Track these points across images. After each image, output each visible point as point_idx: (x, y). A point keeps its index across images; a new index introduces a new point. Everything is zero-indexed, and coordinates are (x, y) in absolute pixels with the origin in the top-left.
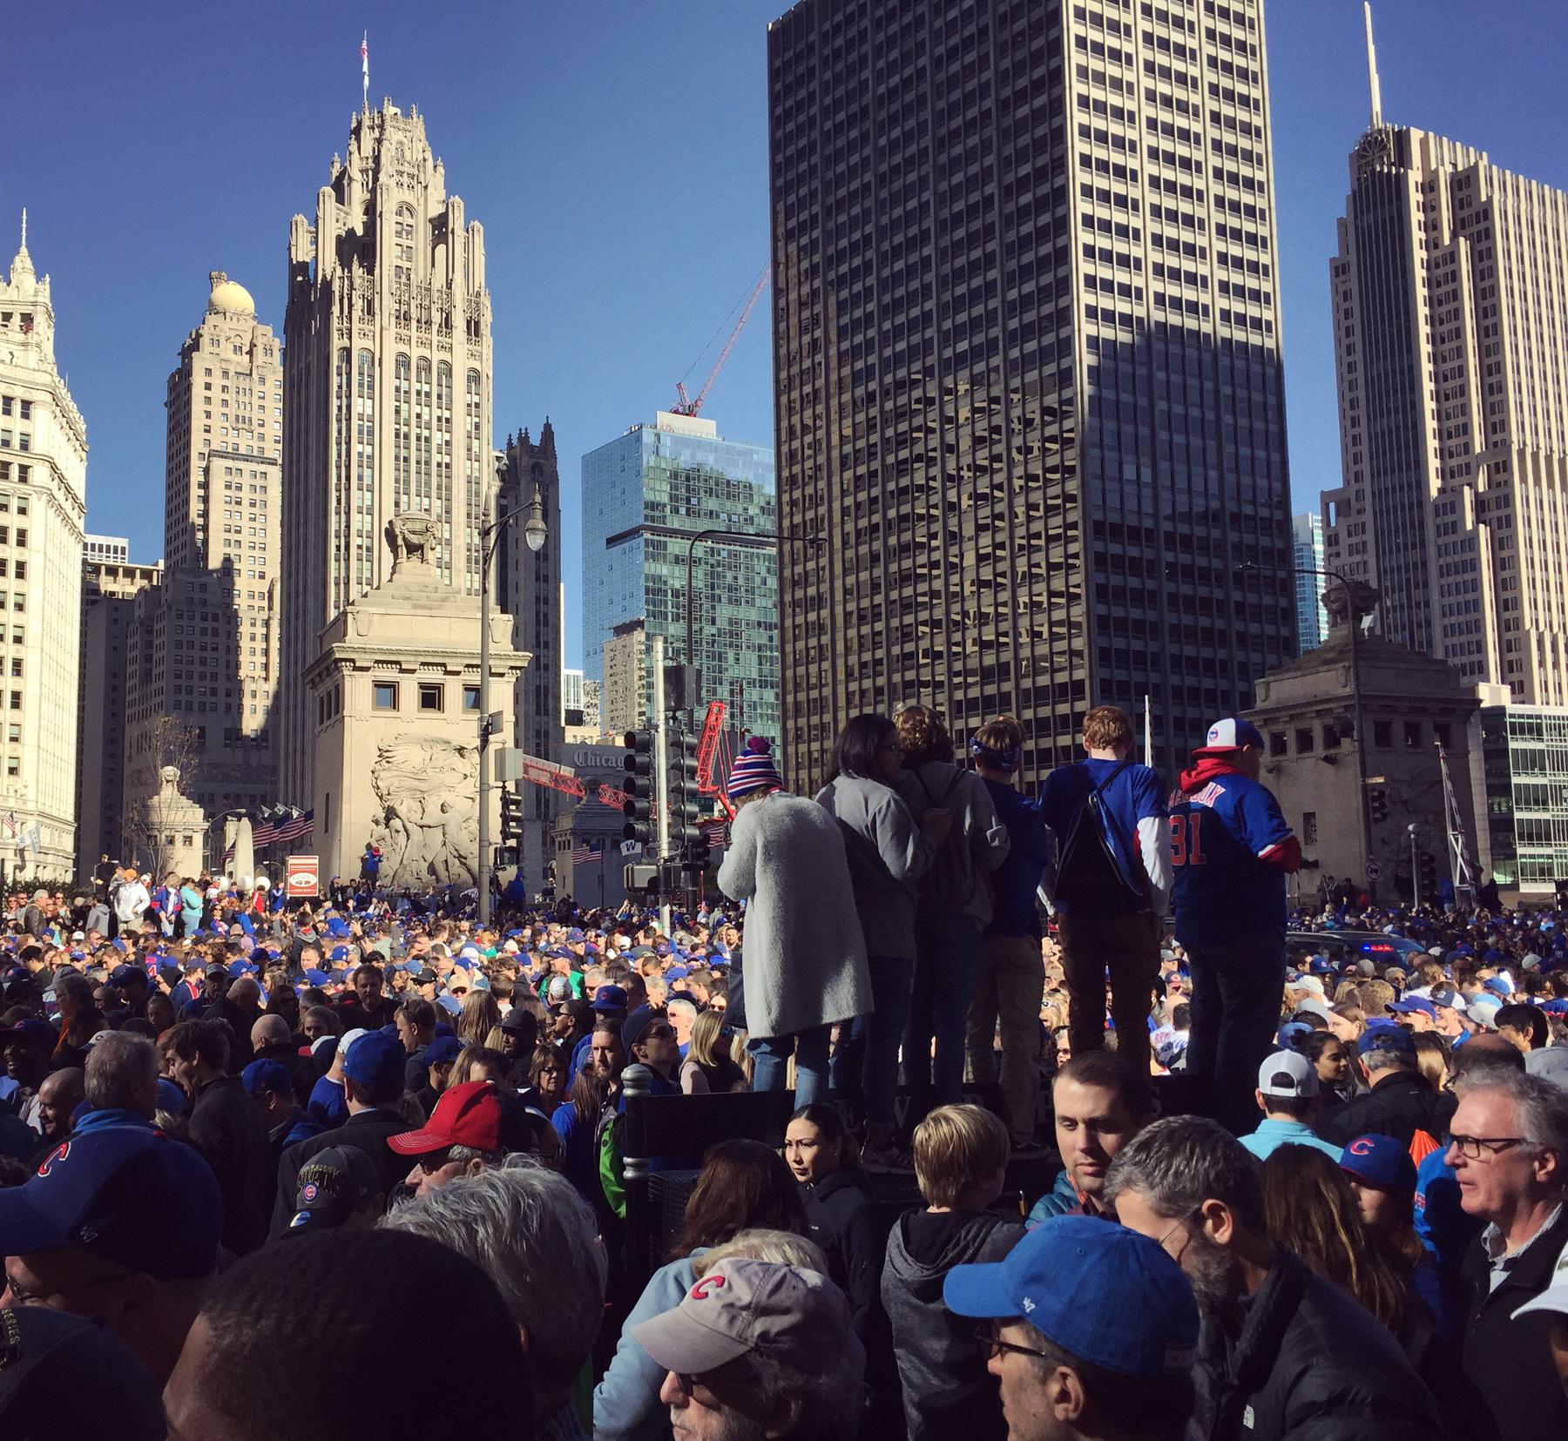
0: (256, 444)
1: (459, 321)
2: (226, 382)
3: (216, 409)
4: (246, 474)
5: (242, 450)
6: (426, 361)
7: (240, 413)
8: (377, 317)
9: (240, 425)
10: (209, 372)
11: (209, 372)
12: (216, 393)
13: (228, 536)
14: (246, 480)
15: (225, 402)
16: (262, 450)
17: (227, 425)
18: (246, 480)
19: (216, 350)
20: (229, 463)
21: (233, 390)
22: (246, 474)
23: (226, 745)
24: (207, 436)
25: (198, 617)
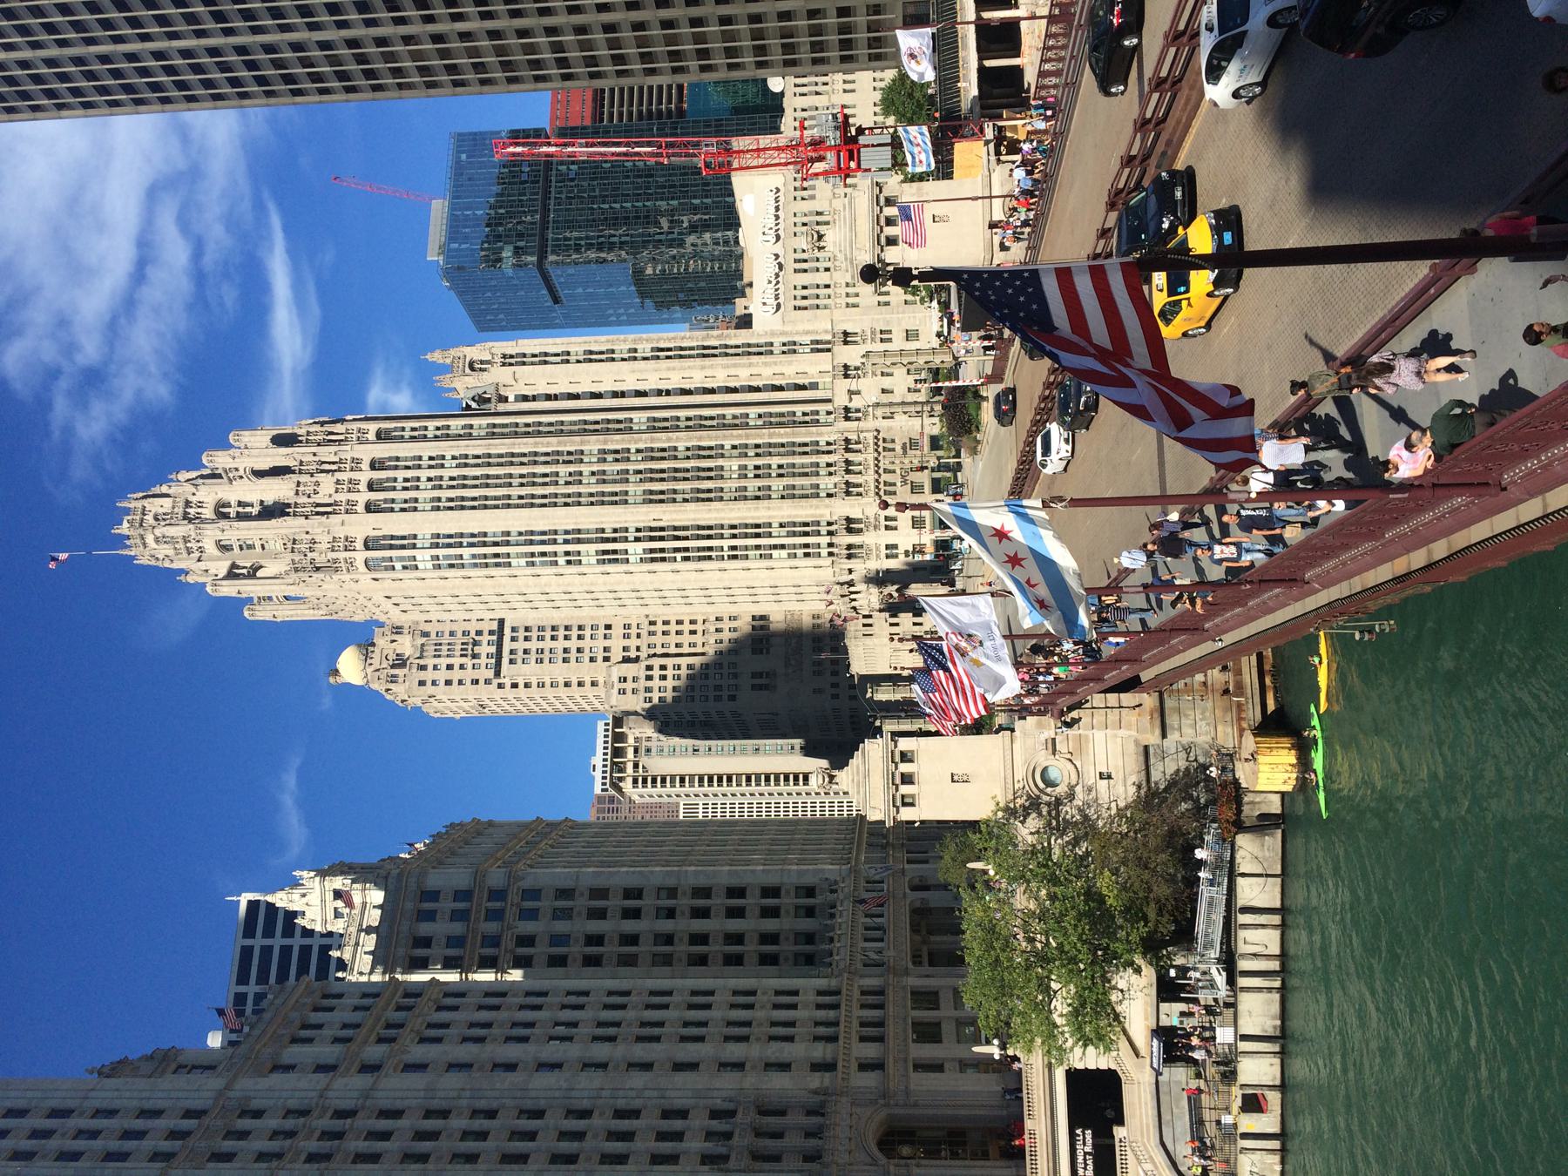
0: (485, 638)
2: (430, 668)
3: (456, 675)
4: (515, 645)
5: (493, 649)
7: (458, 653)
10: (422, 683)
11: (422, 683)
12: (442, 675)
13: (573, 660)
14: (520, 645)
15: (450, 667)
16: (491, 633)
18: (520, 645)
19: (401, 680)
20: (505, 661)
22: (515, 645)
23: (768, 652)
24: (482, 682)
25: (649, 684)
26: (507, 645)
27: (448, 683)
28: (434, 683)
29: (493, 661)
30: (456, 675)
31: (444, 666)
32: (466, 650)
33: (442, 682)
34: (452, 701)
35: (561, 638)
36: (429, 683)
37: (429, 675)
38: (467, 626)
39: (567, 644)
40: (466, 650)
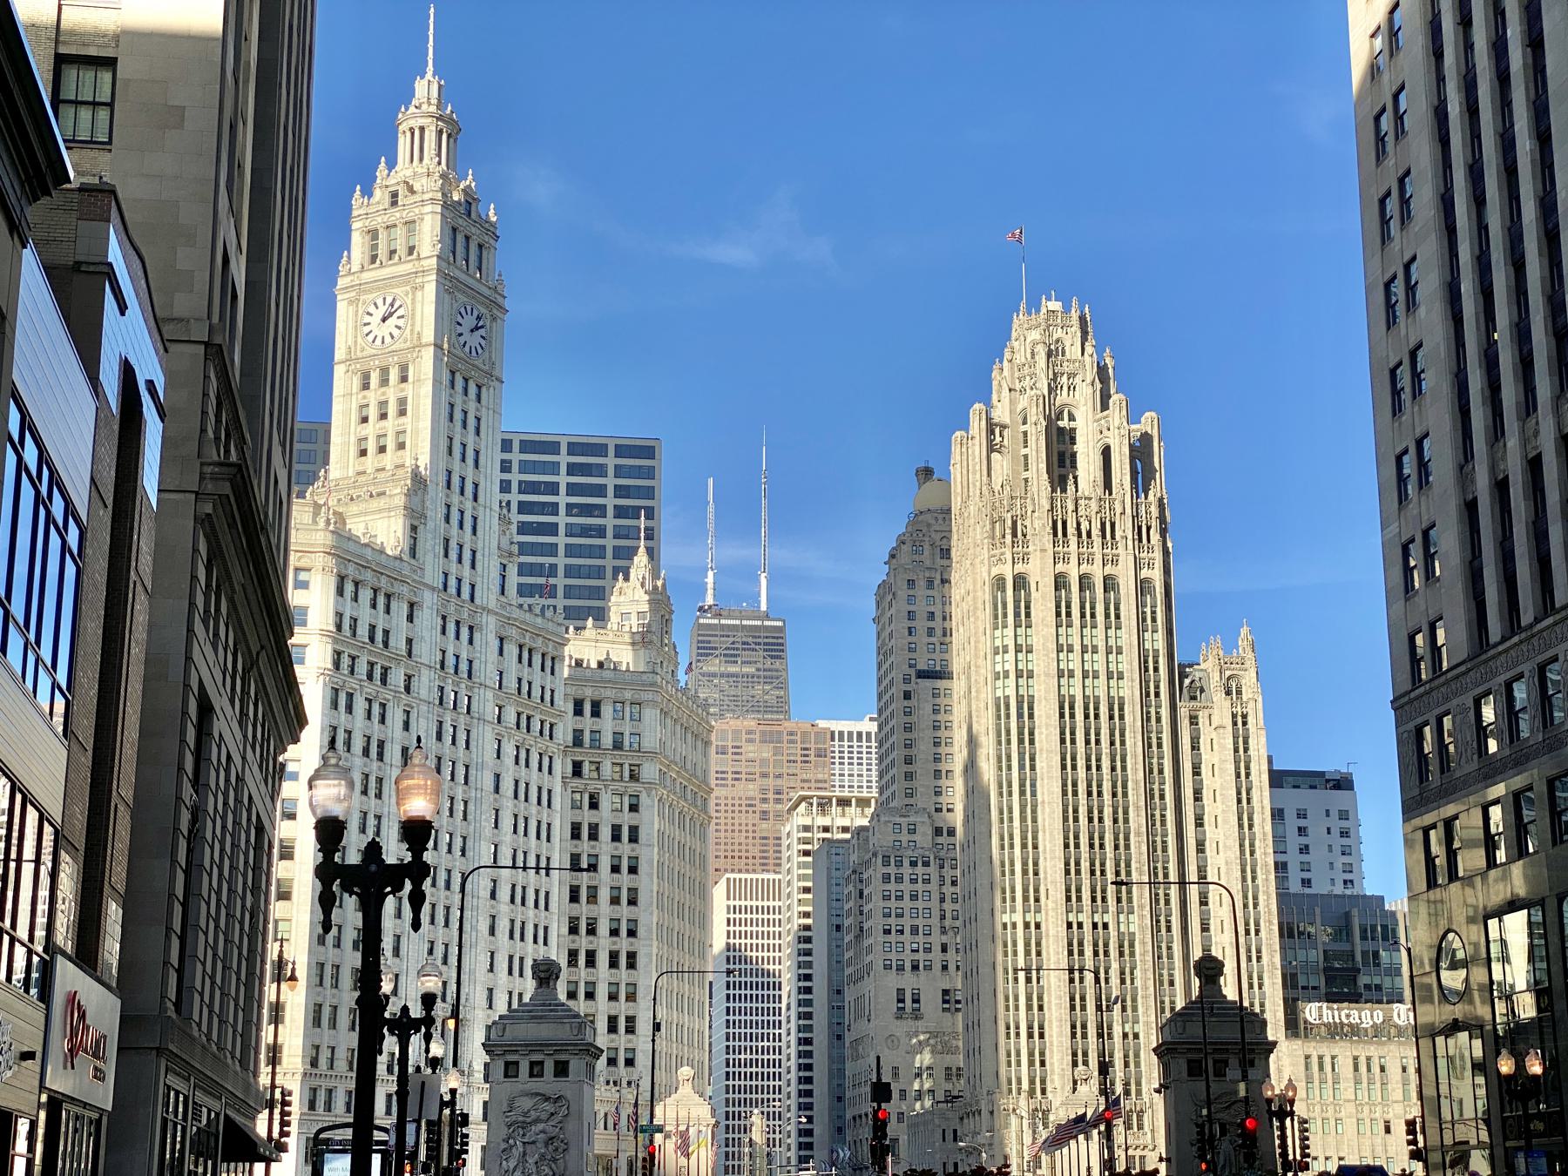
10: (911, 583)
11: (911, 583)
15: (931, 616)
19: (917, 557)
27: (911, 615)
28: (911, 599)
34: (891, 621)
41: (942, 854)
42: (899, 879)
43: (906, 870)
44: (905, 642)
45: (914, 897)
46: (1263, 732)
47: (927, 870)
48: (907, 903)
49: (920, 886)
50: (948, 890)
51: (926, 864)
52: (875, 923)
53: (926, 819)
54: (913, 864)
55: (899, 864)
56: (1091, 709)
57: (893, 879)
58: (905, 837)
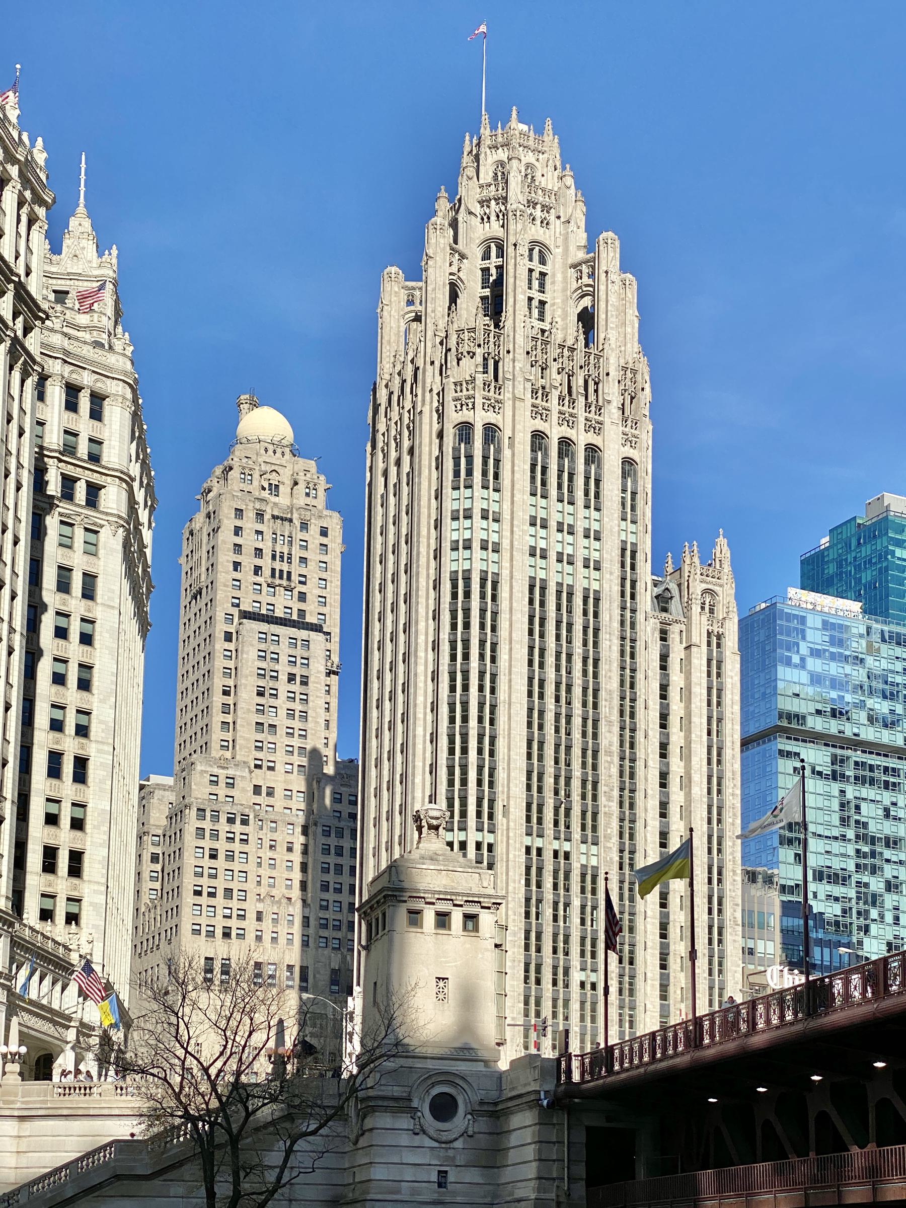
1: (611, 391)
2: (260, 527)
3: (248, 561)
4: (285, 642)
5: (279, 613)
6: (565, 444)
7: (278, 565)
8: (509, 384)
9: (277, 581)
10: (239, 512)
11: (239, 512)
12: (248, 541)
14: (284, 649)
15: (259, 552)
16: (302, 613)
17: (259, 579)
18: (284, 649)
20: (264, 627)
21: (268, 536)
26: (285, 632)
27: (238, 548)
28: (238, 531)
29: (264, 612)
30: (248, 561)
31: (260, 546)
32: (281, 577)
33: (238, 540)
35: (291, 705)
36: (239, 523)
37: (249, 523)
38: (313, 581)
39: (282, 713)
40: (281, 577)
41: (262, 815)
42: (215, 835)
43: (223, 827)
44: (230, 577)
45: (230, 857)
46: (738, 658)
47: (245, 829)
48: (221, 863)
49: (237, 846)
50: (266, 854)
51: (245, 822)
52: (189, 882)
53: (246, 773)
54: (231, 821)
55: (216, 818)
56: (566, 593)
57: (207, 834)
58: (222, 790)
